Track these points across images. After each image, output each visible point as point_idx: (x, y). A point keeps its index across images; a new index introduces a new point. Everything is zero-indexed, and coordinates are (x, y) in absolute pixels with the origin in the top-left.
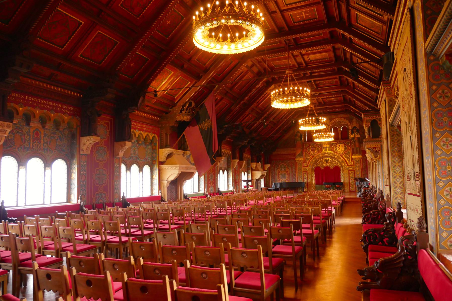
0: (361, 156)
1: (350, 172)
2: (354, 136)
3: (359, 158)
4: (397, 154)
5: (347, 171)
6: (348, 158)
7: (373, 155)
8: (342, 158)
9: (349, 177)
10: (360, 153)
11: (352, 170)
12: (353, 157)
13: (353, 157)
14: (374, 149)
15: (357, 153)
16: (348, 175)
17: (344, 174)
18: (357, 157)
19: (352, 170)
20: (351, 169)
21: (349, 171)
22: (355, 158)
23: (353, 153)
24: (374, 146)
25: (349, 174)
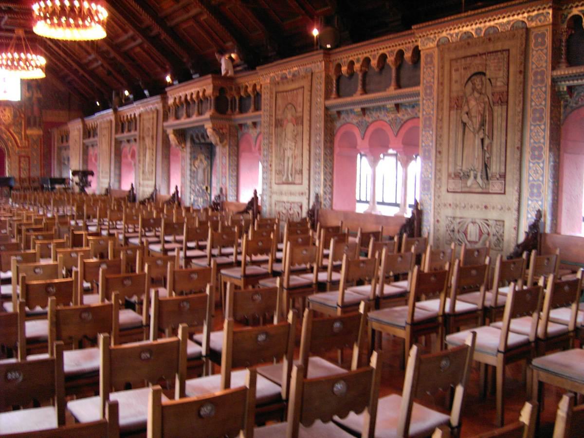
0: (41, 133)
1: (22, 159)
2: (33, 95)
3: (39, 136)
4: (328, 144)
5: (17, 158)
6: (19, 133)
7: (218, 139)
8: (8, 133)
9: (20, 168)
10: (40, 125)
11: (24, 157)
12: (29, 132)
13: (29, 132)
14: (221, 131)
15: (35, 125)
16: (17, 164)
17: (10, 163)
18: (35, 132)
19: (24, 157)
20: (23, 154)
21: (20, 157)
22: (31, 135)
23: (29, 124)
24: (221, 126)
25: (20, 162)
